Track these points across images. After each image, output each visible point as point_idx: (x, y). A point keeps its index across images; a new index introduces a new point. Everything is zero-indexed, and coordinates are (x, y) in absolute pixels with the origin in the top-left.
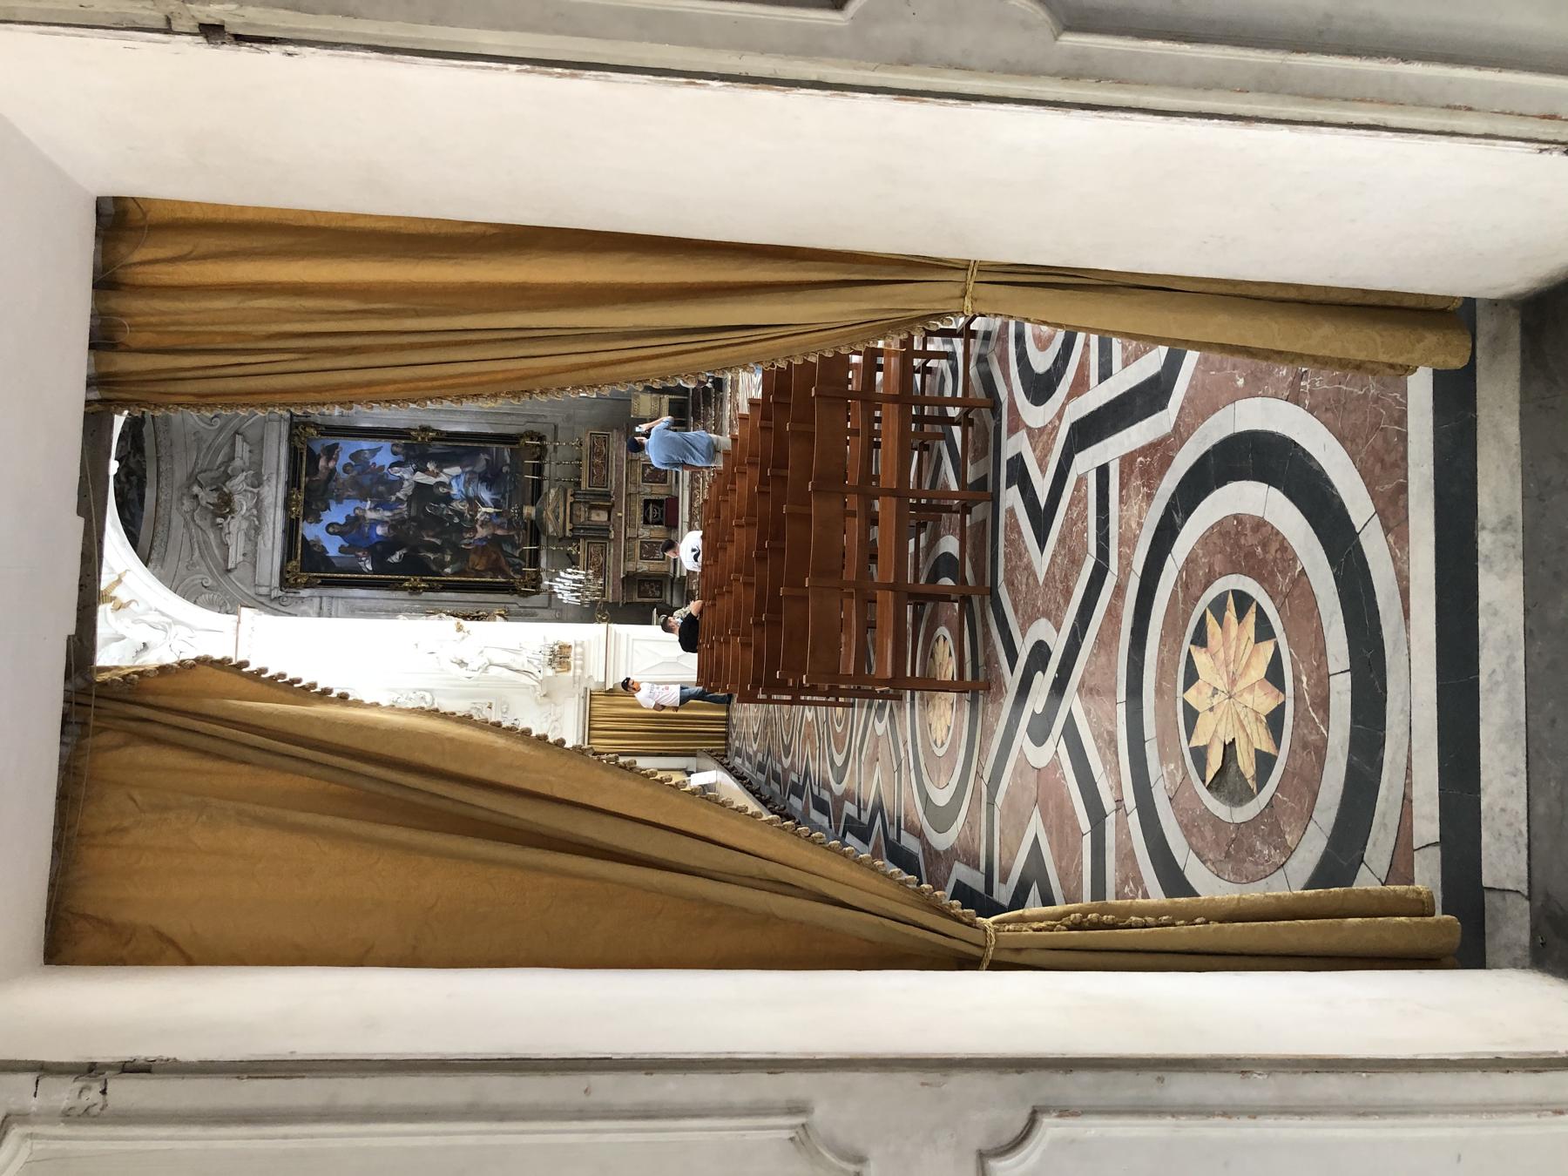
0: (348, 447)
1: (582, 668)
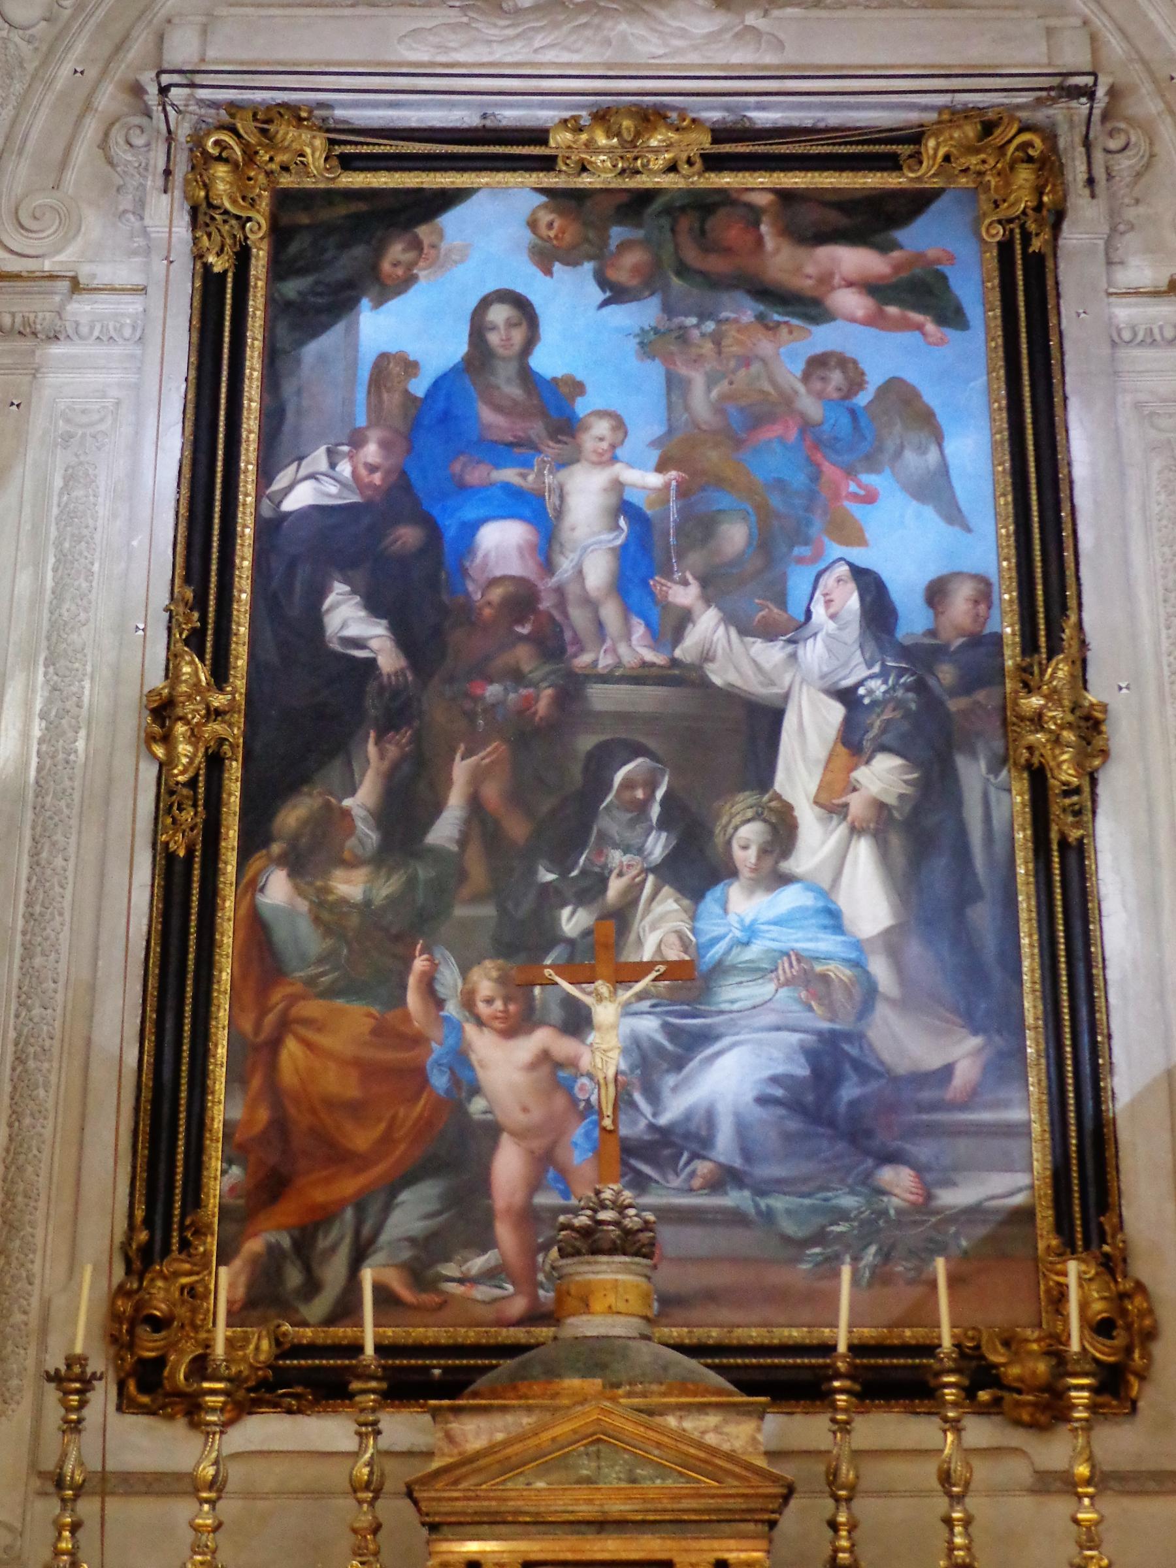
0: (956, 375)
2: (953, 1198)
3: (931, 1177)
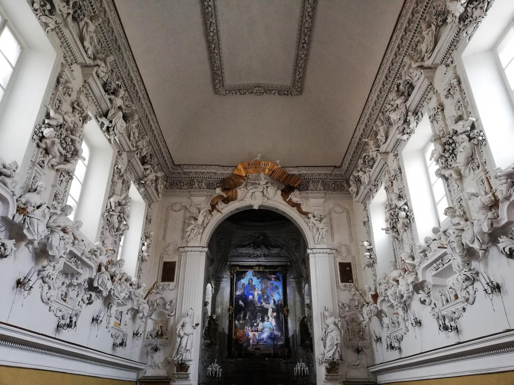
1: (178, 378)
2: (279, 343)
3: (277, 342)
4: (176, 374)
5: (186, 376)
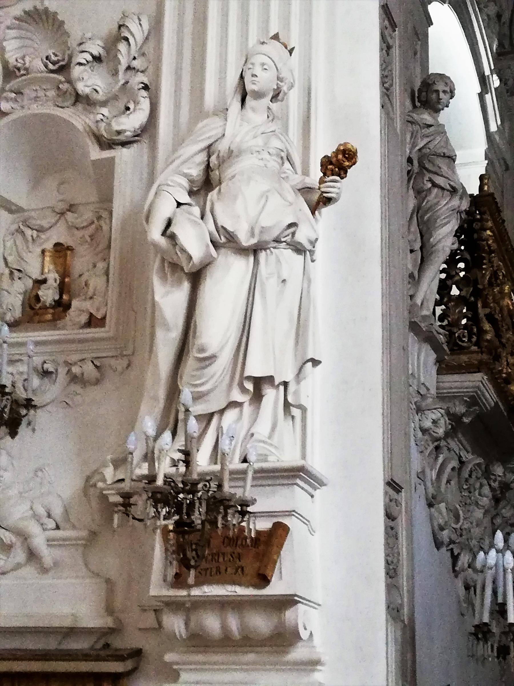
1: (198, 642)
4: (174, 606)
5: (261, 623)
